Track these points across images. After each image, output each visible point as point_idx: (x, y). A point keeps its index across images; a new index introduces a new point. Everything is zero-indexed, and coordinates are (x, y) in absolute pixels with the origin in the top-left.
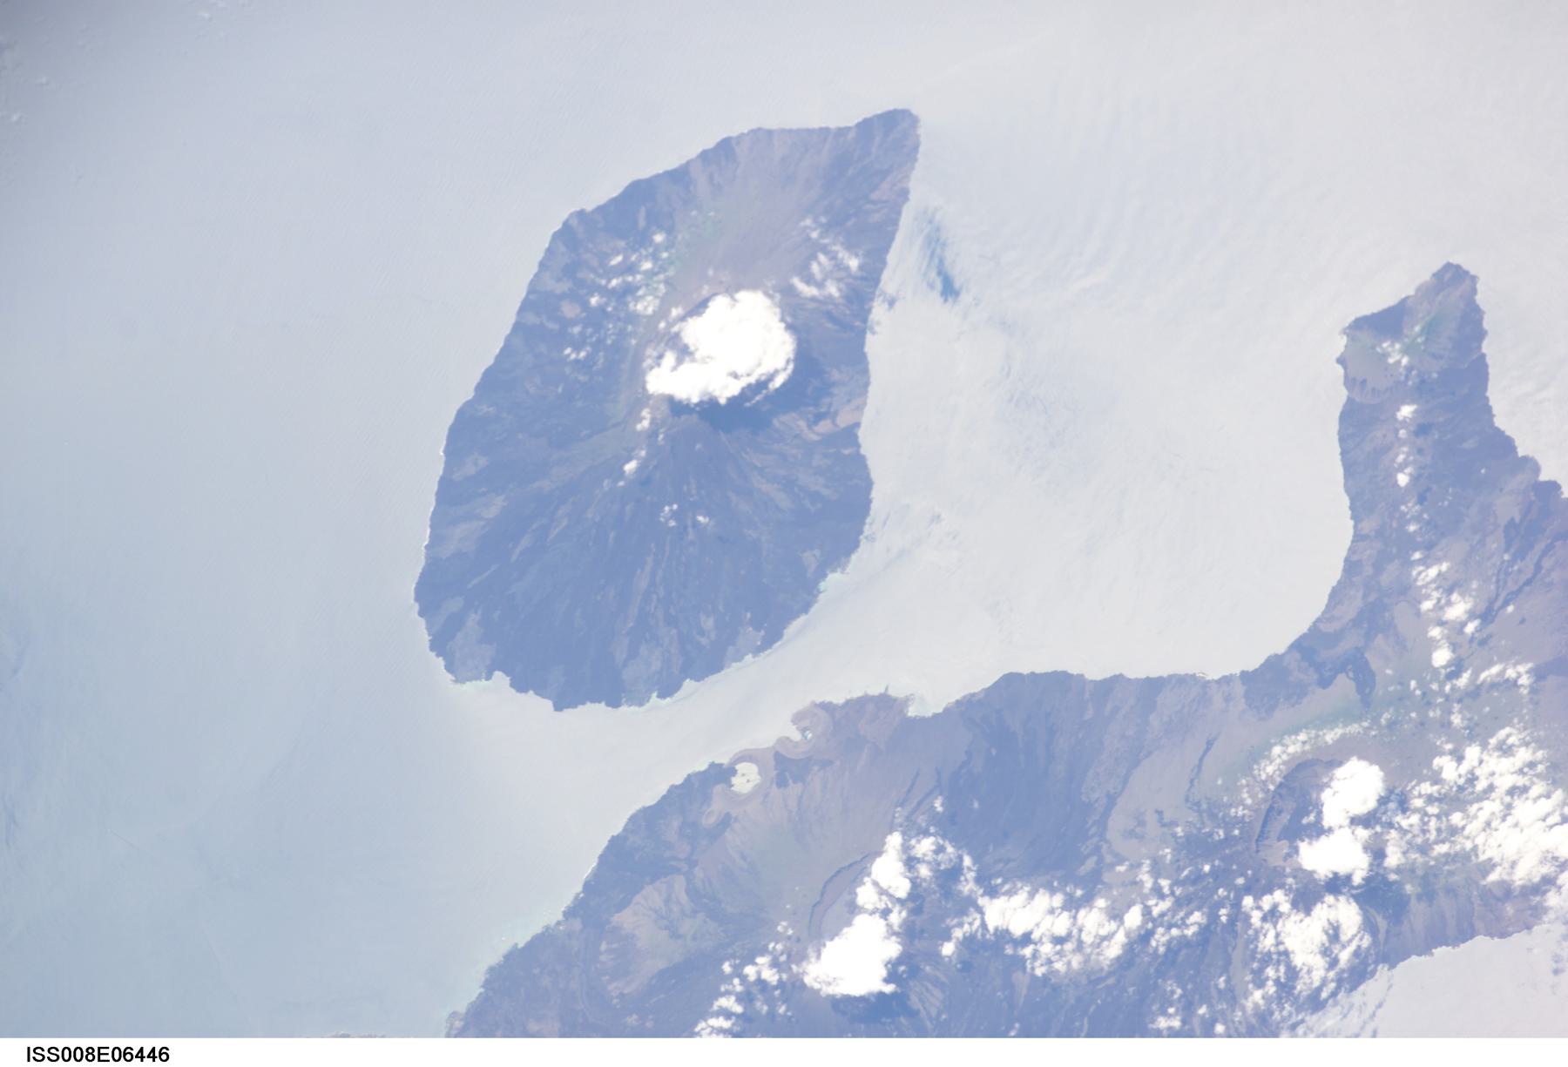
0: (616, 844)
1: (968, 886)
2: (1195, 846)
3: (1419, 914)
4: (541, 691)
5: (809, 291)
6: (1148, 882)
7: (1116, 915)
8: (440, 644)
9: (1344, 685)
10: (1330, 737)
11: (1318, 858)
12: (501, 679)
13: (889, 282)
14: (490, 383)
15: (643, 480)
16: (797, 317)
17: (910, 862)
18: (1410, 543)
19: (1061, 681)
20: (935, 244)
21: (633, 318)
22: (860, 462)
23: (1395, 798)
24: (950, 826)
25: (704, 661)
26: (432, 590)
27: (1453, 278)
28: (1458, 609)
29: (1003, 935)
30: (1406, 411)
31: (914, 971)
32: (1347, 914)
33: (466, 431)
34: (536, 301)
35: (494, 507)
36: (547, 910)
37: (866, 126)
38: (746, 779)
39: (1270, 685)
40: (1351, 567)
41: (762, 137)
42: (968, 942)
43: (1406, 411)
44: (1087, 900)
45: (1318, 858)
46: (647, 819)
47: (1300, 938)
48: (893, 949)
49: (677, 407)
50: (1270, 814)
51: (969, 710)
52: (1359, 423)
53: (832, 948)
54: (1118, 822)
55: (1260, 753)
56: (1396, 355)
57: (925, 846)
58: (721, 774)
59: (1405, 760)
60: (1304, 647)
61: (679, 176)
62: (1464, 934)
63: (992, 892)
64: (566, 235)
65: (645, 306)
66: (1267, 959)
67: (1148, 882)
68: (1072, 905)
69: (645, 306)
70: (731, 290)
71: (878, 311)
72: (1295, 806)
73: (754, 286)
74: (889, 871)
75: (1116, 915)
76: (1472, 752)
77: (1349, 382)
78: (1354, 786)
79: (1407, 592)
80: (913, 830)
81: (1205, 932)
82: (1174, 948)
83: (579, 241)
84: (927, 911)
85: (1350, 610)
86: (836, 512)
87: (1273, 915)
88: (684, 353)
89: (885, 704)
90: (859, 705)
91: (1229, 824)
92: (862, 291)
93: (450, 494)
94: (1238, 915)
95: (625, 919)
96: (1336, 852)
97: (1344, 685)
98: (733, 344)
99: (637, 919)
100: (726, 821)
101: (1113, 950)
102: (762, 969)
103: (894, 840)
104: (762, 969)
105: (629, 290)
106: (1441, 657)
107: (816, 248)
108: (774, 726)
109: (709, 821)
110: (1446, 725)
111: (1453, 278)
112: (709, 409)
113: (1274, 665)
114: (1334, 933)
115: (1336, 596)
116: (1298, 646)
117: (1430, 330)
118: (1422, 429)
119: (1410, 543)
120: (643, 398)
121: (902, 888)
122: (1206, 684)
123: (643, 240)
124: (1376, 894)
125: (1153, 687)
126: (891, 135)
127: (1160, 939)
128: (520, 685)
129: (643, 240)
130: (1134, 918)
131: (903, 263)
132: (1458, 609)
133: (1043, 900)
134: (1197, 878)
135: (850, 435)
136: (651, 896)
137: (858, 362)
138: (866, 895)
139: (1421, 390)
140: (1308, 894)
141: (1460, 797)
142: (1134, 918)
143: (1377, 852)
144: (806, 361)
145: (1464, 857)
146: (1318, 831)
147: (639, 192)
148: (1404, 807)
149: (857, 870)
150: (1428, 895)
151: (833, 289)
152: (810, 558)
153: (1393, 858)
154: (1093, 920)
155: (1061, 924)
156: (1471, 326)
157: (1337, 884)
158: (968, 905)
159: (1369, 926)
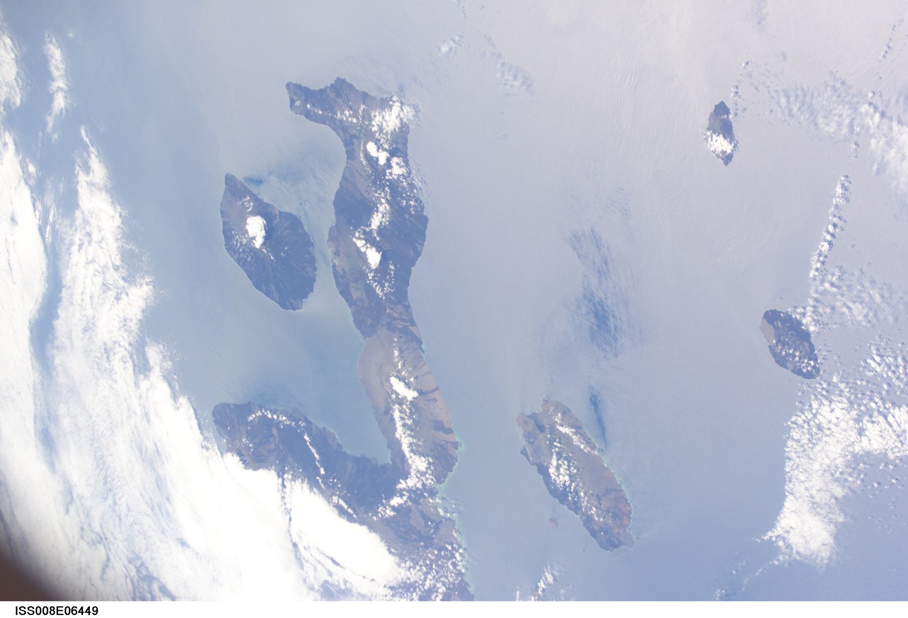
0: (340, 292)
1: (367, 229)
2: (374, 183)
3: (400, 146)
4: (308, 293)
5: (250, 209)
6: (377, 195)
7: (381, 204)
8: (294, 309)
9: (355, 141)
10: (362, 148)
11: (382, 161)
12: (304, 300)
13: (256, 192)
14: (250, 276)
15: (275, 256)
16: (254, 213)
17: (359, 238)
18: (332, 116)
19: (337, 194)
20: (250, 180)
21: (246, 244)
22: (286, 213)
23: (377, 142)
24: (356, 229)
25: (313, 261)
26: (284, 306)
27: (289, 86)
28: (347, 113)
29: (379, 227)
30: (308, 106)
31: (380, 247)
32: (395, 160)
33: (257, 285)
34: (238, 261)
35: (273, 287)
36: (349, 311)
37: (226, 184)
38: (337, 262)
39: (351, 155)
40: (334, 129)
41: (222, 204)
42: (378, 234)
43: (308, 106)
44: (378, 208)
45: (382, 161)
46: (338, 284)
47: (397, 170)
48: (374, 249)
49: (264, 244)
50: (372, 166)
51: (338, 213)
52: (308, 115)
53: (370, 261)
54: (366, 195)
55: (361, 162)
56: (298, 103)
57: (357, 234)
58: (334, 266)
59: (370, 136)
60: (346, 145)
61: (224, 223)
62: (406, 139)
63: (370, 225)
64: (228, 250)
65: (245, 241)
66: (398, 179)
67: (377, 195)
68: (377, 211)
69: (245, 241)
70: (246, 224)
71: (260, 197)
72: (372, 161)
73: (246, 220)
74: (360, 243)
75: (381, 204)
76: (373, 123)
77: (301, 114)
78: (371, 148)
79: (341, 121)
80: (354, 236)
81: (390, 188)
82: (392, 196)
83: (230, 248)
84: (369, 239)
85: (342, 133)
86: (294, 221)
87: (391, 174)
88: (254, 238)
89: (331, 229)
90: (330, 235)
91: (371, 175)
92: (255, 198)
93: (268, 294)
94: (389, 180)
95: (354, 297)
96: (382, 157)
97: (355, 141)
98: (255, 227)
99: (355, 295)
100: (343, 270)
101: (388, 207)
102: (371, 275)
103: (354, 239)
104: (371, 275)
105: (241, 243)
106: (355, 120)
107: (243, 204)
108: (329, 251)
109: (342, 273)
110: (367, 126)
111: (289, 86)
112: (267, 238)
113: (348, 152)
114: (398, 164)
115: (338, 135)
116: (345, 146)
117: (296, 95)
118: (313, 105)
119: (332, 116)
120: (260, 249)
121: (363, 242)
122: (347, 167)
123: (233, 235)
124: (393, 153)
125: (344, 177)
126: (229, 179)
127: (388, 197)
128: (306, 297)
129: (233, 235)
130: (383, 201)
131: (253, 188)
132: (347, 113)
133: (375, 216)
134: (380, 185)
135: (281, 213)
136: (352, 290)
137: (267, 205)
138: (363, 250)
139: (306, 101)
140: (389, 165)
141: (381, 129)
142: (383, 201)
143: (385, 150)
144: (264, 215)
145: (392, 133)
146: (377, 159)
147: (225, 232)
148: (379, 140)
149: (358, 249)
150: (397, 143)
151: (252, 204)
152: (300, 231)
153: (387, 147)
154: (381, 209)
155: (380, 215)
156: (298, 86)
157: (388, 160)
158: (371, 232)
159: (398, 157)
